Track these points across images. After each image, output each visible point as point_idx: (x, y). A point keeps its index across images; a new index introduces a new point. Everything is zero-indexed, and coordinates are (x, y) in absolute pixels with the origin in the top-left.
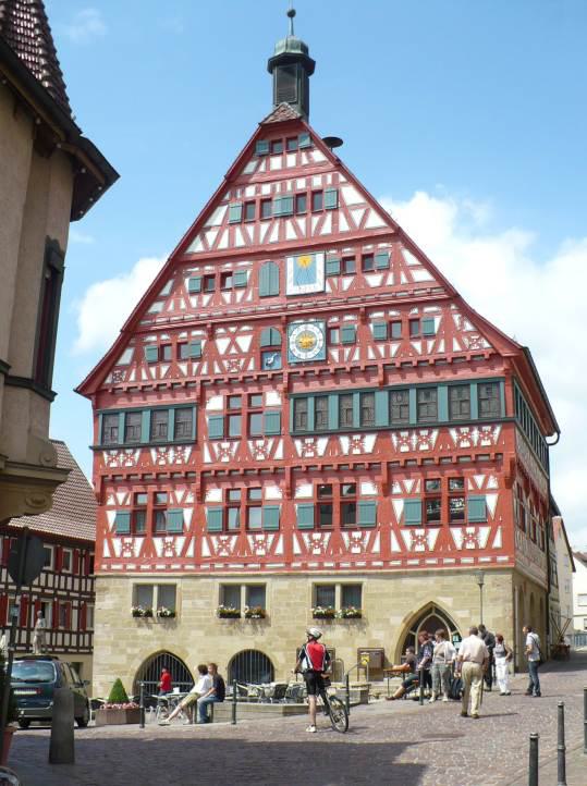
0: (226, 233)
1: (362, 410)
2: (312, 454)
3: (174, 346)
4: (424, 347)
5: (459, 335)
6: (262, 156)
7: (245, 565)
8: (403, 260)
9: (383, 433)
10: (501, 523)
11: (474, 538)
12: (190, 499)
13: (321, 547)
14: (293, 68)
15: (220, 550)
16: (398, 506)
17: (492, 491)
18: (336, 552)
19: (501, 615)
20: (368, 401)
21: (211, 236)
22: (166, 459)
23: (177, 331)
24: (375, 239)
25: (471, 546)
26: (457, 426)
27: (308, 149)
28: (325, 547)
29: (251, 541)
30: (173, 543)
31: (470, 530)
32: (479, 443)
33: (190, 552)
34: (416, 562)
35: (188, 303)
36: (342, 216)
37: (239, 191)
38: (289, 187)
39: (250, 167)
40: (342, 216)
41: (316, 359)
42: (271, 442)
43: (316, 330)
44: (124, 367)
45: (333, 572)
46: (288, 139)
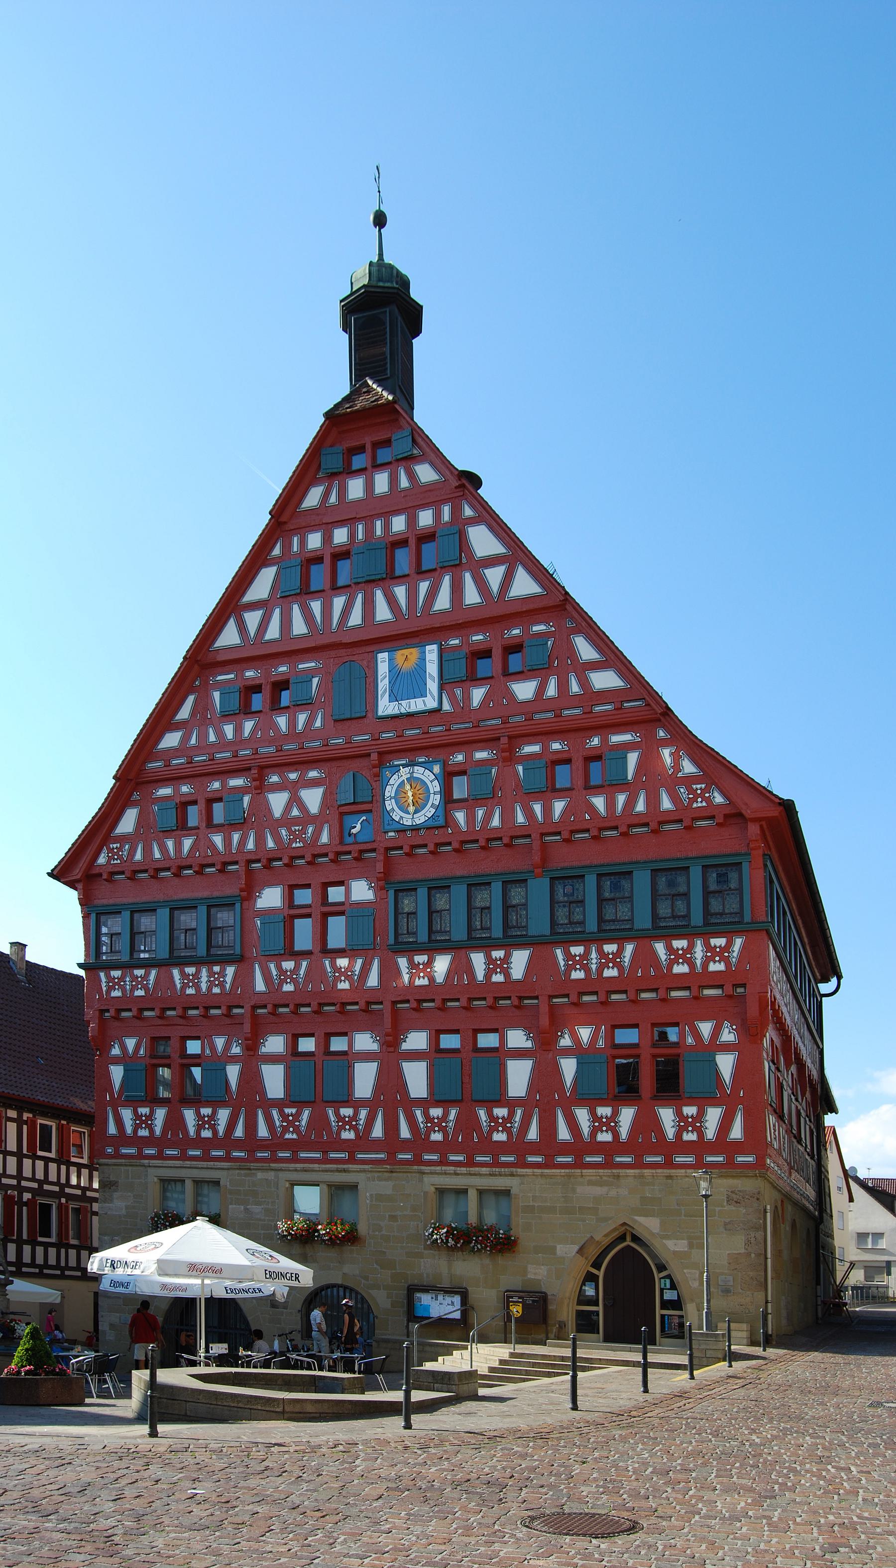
0: (277, 612)
1: (507, 907)
2: (425, 982)
3: (202, 804)
4: (611, 804)
5: (674, 782)
6: (333, 475)
7: (325, 1152)
8: (572, 653)
9: (541, 945)
10: (741, 1101)
11: (697, 1124)
12: (236, 1050)
13: (443, 1130)
14: (382, 318)
15: (285, 1130)
16: (569, 1067)
17: (727, 1048)
18: (468, 1137)
19: (743, 1251)
20: (517, 895)
21: (252, 619)
22: (197, 986)
24: (528, 611)
26: (667, 938)
27: (408, 460)
28: (451, 1131)
29: (332, 1118)
31: (690, 1111)
32: (705, 965)
33: (239, 1132)
34: (598, 1159)
35: (220, 733)
36: (468, 577)
38: (379, 532)
39: (313, 498)
40: (468, 577)
41: (431, 823)
42: (359, 962)
43: (429, 777)
44: (123, 839)
45: (464, 1170)
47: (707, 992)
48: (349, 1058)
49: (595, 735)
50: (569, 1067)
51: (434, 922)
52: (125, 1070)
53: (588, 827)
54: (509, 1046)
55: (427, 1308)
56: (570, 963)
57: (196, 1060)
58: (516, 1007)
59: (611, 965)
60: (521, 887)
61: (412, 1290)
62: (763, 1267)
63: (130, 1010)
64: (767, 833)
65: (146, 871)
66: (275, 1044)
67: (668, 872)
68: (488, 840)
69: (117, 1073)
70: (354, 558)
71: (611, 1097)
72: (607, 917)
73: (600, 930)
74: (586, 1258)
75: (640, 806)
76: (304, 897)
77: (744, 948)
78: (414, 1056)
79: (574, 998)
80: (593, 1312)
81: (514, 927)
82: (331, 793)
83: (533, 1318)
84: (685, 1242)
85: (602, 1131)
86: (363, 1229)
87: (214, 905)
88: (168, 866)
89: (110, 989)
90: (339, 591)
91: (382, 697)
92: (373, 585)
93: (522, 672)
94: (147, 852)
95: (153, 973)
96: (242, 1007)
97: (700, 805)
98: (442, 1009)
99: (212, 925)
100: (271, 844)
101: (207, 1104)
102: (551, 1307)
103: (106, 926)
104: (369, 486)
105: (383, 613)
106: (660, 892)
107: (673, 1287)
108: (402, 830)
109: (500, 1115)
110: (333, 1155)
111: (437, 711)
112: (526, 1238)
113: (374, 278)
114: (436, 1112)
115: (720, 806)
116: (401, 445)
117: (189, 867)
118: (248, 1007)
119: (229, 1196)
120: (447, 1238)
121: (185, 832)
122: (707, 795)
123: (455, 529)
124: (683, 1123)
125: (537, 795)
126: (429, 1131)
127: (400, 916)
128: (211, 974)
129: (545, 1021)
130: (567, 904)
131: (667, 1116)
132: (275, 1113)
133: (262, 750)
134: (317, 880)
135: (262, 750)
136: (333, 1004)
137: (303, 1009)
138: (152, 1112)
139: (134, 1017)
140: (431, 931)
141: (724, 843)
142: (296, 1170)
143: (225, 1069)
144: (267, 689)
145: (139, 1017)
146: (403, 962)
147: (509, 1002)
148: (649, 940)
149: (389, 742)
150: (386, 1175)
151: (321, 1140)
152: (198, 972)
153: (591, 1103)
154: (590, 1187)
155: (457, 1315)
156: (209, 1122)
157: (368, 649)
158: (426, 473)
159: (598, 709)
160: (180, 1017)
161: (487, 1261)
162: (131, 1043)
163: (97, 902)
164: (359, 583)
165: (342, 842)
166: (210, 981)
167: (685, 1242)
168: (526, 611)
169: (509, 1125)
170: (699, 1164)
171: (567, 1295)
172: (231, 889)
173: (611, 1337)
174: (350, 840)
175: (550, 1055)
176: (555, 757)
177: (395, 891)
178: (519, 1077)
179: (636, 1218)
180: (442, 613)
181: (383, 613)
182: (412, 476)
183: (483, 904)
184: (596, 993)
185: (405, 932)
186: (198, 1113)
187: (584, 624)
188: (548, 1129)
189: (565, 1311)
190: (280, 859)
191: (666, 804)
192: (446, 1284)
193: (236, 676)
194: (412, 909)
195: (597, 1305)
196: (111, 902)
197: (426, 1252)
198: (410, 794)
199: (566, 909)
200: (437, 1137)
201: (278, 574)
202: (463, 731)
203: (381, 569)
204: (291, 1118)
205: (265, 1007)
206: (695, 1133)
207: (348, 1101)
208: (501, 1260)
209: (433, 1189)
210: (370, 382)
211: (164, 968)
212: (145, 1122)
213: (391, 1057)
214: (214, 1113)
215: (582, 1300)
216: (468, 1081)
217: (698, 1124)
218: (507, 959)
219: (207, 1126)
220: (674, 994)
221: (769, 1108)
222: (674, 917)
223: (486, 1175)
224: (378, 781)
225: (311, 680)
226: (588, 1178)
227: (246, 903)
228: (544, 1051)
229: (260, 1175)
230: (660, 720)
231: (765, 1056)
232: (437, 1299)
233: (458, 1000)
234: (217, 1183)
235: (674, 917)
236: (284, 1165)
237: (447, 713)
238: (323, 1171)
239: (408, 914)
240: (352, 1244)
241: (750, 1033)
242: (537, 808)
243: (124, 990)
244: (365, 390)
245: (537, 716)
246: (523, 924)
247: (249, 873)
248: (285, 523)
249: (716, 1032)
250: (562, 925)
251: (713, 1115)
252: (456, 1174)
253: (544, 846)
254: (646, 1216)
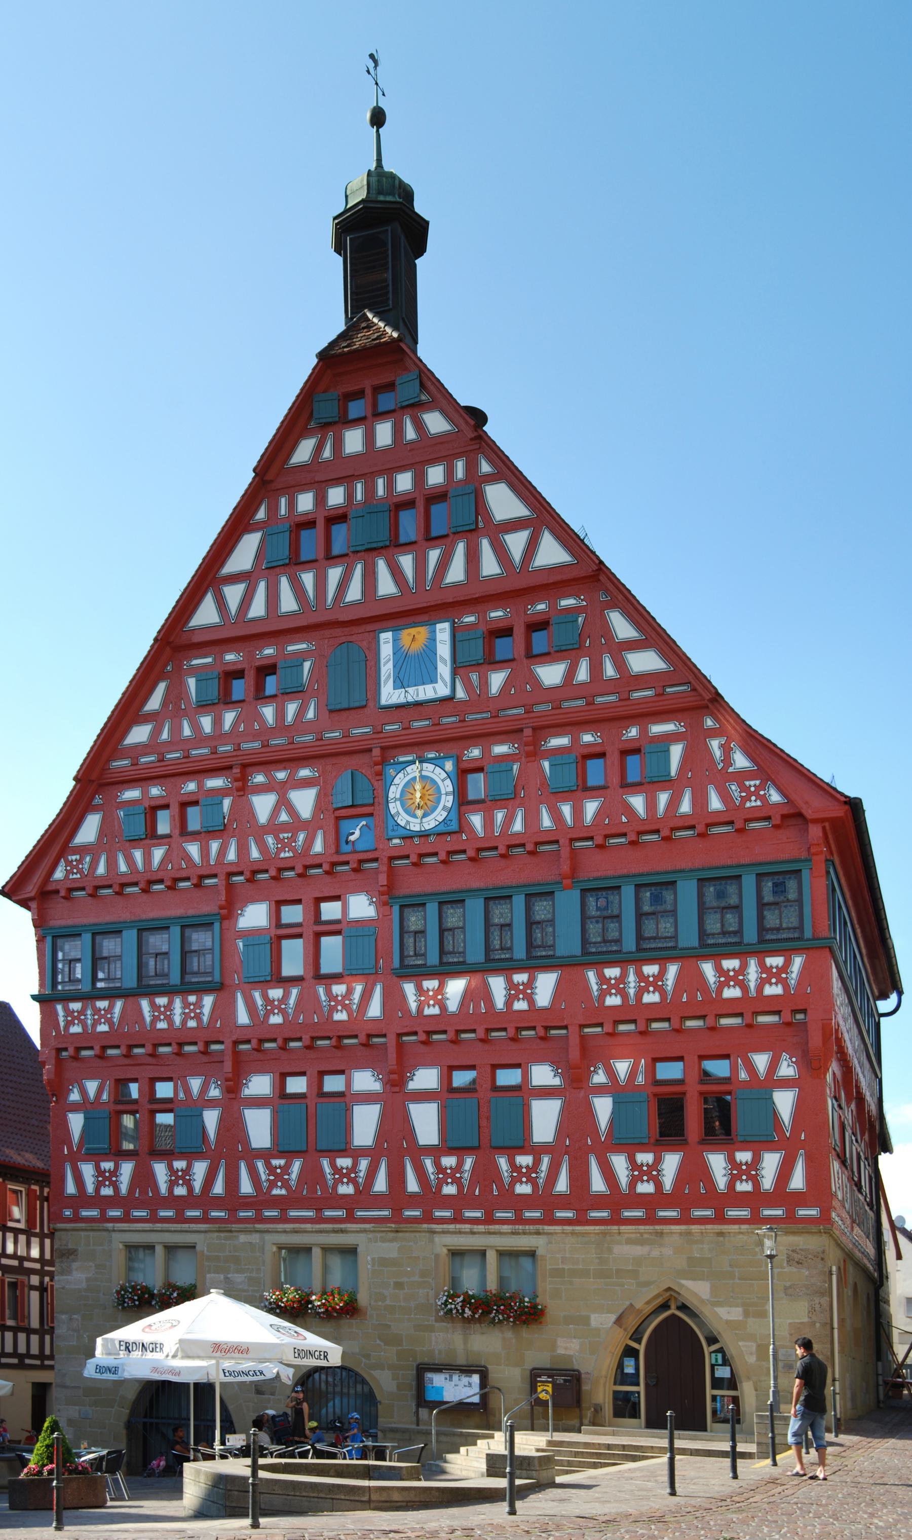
0: (262, 587)
1: (531, 924)
2: (436, 1011)
3: (175, 808)
4: (651, 805)
5: (724, 777)
6: (325, 426)
7: (319, 1210)
8: (607, 630)
11: (752, 1171)
12: (214, 1093)
13: (458, 1182)
15: (272, 1184)
16: (603, 1107)
17: (785, 1084)
19: (806, 1320)
20: (541, 910)
21: (233, 594)
22: (170, 1020)
23: (179, 779)
24: (554, 583)
25: (744, 1187)
26: (717, 957)
27: (415, 408)
28: (466, 1183)
29: (327, 1169)
30: (188, 1171)
31: (744, 1156)
33: (218, 1188)
34: (638, 1213)
36: (485, 544)
37: (283, 501)
38: (381, 491)
39: (303, 452)
40: (485, 544)
41: (442, 829)
42: (359, 989)
44: (83, 850)
45: (481, 1228)
46: (378, 390)
47: (763, 1019)
48: (346, 1100)
49: (633, 725)
50: (603, 1107)
51: (446, 943)
52: (85, 1118)
53: (625, 830)
54: (534, 1083)
55: (440, 1390)
56: (605, 987)
57: (167, 1105)
58: (542, 1038)
59: (651, 989)
60: (545, 900)
61: (422, 1370)
62: (829, 1339)
63: (91, 1048)
64: (830, 836)
65: (110, 886)
66: (260, 1085)
67: (717, 881)
68: (509, 847)
69: (76, 1122)
70: (352, 522)
71: (652, 1141)
72: (647, 934)
73: (639, 949)
74: (625, 1330)
75: (685, 807)
76: (293, 914)
77: (804, 968)
78: (424, 1096)
79: (608, 1028)
80: (632, 1393)
81: (539, 947)
82: (325, 794)
83: (564, 1398)
84: (740, 1310)
85: (642, 1181)
86: (363, 1299)
87: (188, 925)
88: (135, 880)
89: (68, 1024)
90: (335, 560)
91: (385, 683)
92: (375, 553)
93: (548, 654)
94: (112, 864)
95: (119, 1005)
96: (222, 1043)
97: (753, 804)
98: (455, 1042)
99: (187, 949)
100: (255, 854)
101: (182, 1156)
102: (585, 1387)
103: (62, 950)
104: (370, 438)
105: (386, 586)
106: (708, 905)
107: (726, 1362)
108: (408, 837)
109: (524, 1164)
110: (328, 1213)
111: (450, 699)
112: (554, 1307)
113: (374, 191)
114: (449, 1161)
115: (776, 805)
116: (407, 390)
117: (161, 881)
118: (229, 1042)
119: (207, 1263)
120: (463, 1307)
121: (155, 841)
122: (762, 793)
123: (470, 488)
124: (736, 1171)
125: (567, 794)
126: (441, 1183)
127: (406, 936)
128: (186, 1005)
129: (574, 1053)
130: (600, 920)
131: (717, 1163)
132: (260, 1165)
133: (244, 746)
134: (308, 895)
135: (244, 746)
136: (329, 1038)
137: (293, 1044)
138: (117, 1167)
139: (96, 1056)
140: (442, 952)
141: (782, 847)
142: (285, 1232)
143: (201, 1115)
144: (250, 675)
145: (101, 1056)
146: (409, 989)
147: (532, 1033)
148: (695, 959)
149: (393, 735)
150: (391, 1235)
151: (315, 1196)
152: (171, 1002)
153: (630, 1149)
154: (628, 1247)
155: (476, 1399)
156: (183, 1178)
157: (369, 627)
158: (436, 423)
159: (636, 695)
160: (150, 1055)
161: (509, 1334)
162: (92, 1086)
163: (52, 923)
164: (358, 552)
165: (338, 851)
166: (184, 1013)
167: (740, 1310)
168: (554, 583)
169: (534, 1175)
170: (756, 1219)
171: (604, 1373)
172: (208, 907)
173: (655, 1422)
174: (348, 848)
175: (582, 1094)
176: (585, 751)
177: (402, 907)
178: (545, 1119)
179: (684, 1282)
180: (456, 586)
181: (386, 586)
182: (419, 426)
183: (502, 921)
184: (634, 1021)
185: (412, 953)
186: (170, 1167)
187: (620, 597)
188: (580, 1178)
189: (601, 1392)
190: (266, 871)
191: (715, 803)
192: (461, 1361)
193: (215, 659)
194: (420, 927)
195: (638, 1384)
196: (70, 922)
197: (437, 1324)
198: (418, 795)
199: (600, 925)
200: (450, 1190)
201: (262, 541)
202: (481, 722)
203: (384, 536)
204: (279, 1171)
205: (248, 1042)
206: (750, 1183)
207: (345, 1150)
208: (526, 1333)
209: (445, 1251)
210: (370, 315)
211: (131, 999)
212: (109, 1179)
213: (395, 1098)
214: (189, 1166)
215: (622, 1377)
216: (486, 1123)
217: (753, 1173)
218: (530, 984)
219: (181, 1182)
220: (724, 1021)
221: (833, 1152)
222: (724, 933)
223: (508, 1233)
224: (380, 778)
225: (302, 665)
226: (627, 1236)
227: (226, 922)
228: (575, 1090)
229: (243, 1238)
230: (707, 707)
231: (828, 1092)
232: (451, 1380)
233: (474, 1031)
234: (193, 1247)
235: (724, 933)
236: (271, 1226)
237: (462, 702)
238: (316, 1232)
239: (416, 933)
240: (352, 1316)
241: (812, 1066)
242: (566, 810)
243: (85, 1026)
244: (364, 325)
245: (566, 704)
246: (550, 943)
247: (230, 887)
248: (271, 481)
249: (773, 1066)
250: (595, 943)
251: (771, 1162)
252: (472, 1233)
253: (574, 853)
254: (694, 1279)
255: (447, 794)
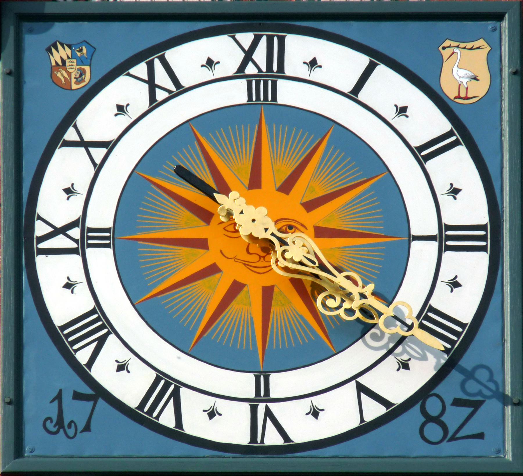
255: (448, 238)
